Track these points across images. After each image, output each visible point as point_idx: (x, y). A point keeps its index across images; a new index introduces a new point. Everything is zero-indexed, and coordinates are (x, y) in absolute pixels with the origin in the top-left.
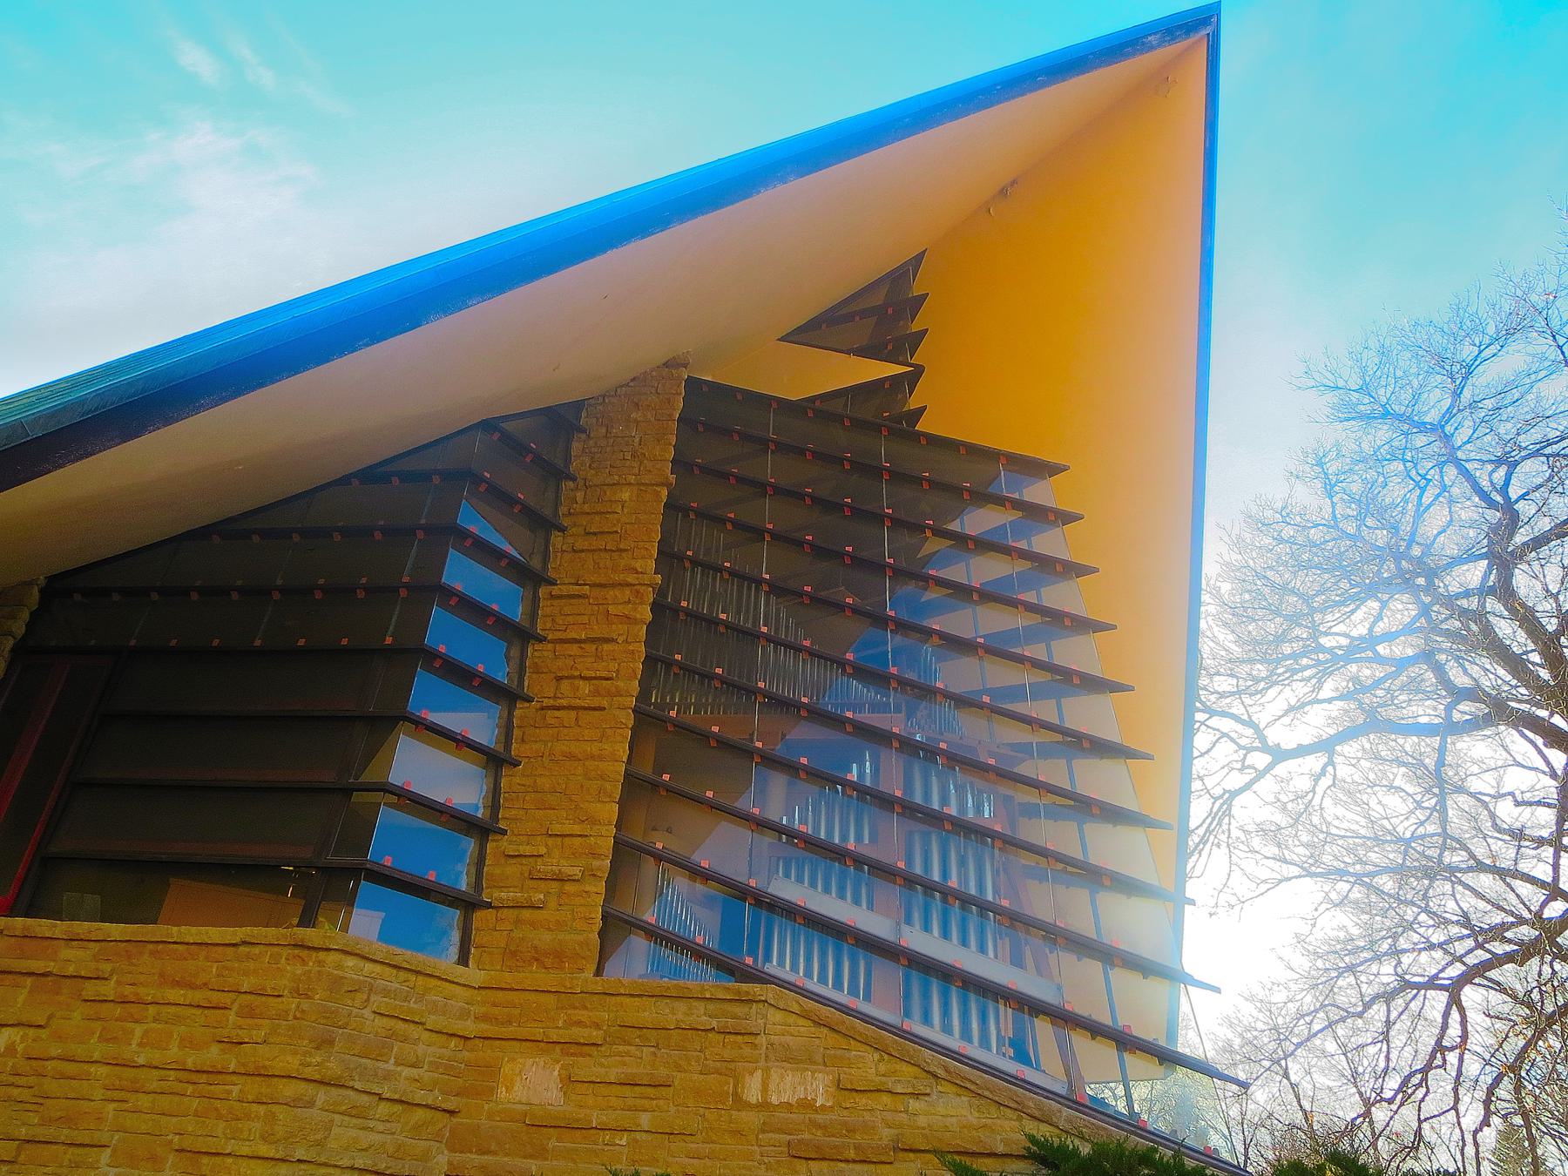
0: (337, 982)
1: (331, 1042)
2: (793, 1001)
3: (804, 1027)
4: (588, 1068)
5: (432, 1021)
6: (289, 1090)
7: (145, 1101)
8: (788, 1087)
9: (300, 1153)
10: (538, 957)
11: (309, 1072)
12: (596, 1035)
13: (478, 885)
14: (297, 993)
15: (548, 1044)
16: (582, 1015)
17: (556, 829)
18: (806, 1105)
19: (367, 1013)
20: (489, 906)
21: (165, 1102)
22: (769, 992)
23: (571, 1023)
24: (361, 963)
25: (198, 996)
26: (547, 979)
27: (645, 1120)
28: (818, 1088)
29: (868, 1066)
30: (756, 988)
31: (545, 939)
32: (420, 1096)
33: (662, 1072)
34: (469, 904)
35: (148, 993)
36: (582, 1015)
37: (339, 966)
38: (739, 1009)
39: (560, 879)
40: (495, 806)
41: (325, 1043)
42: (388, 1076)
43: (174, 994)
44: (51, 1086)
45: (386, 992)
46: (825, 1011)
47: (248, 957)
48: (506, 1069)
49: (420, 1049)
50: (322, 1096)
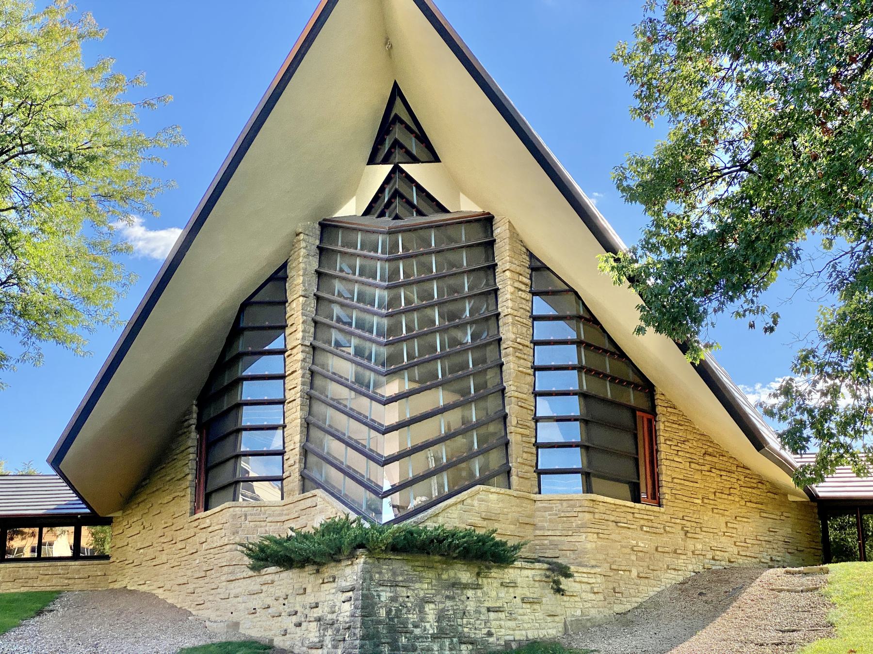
0: (234, 516)
1: (238, 533)
5: (267, 520)
6: (228, 547)
9: (234, 563)
11: (231, 542)
12: (296, 515)
19: (247, 522)
24: (240, 509)
34: (281, 479)
36: (297, 509)
37: (234, 511)
38: (313, 498)
41: (235, 533)
45: (251, 515)
47: (223, 514)
49: (267, 529)
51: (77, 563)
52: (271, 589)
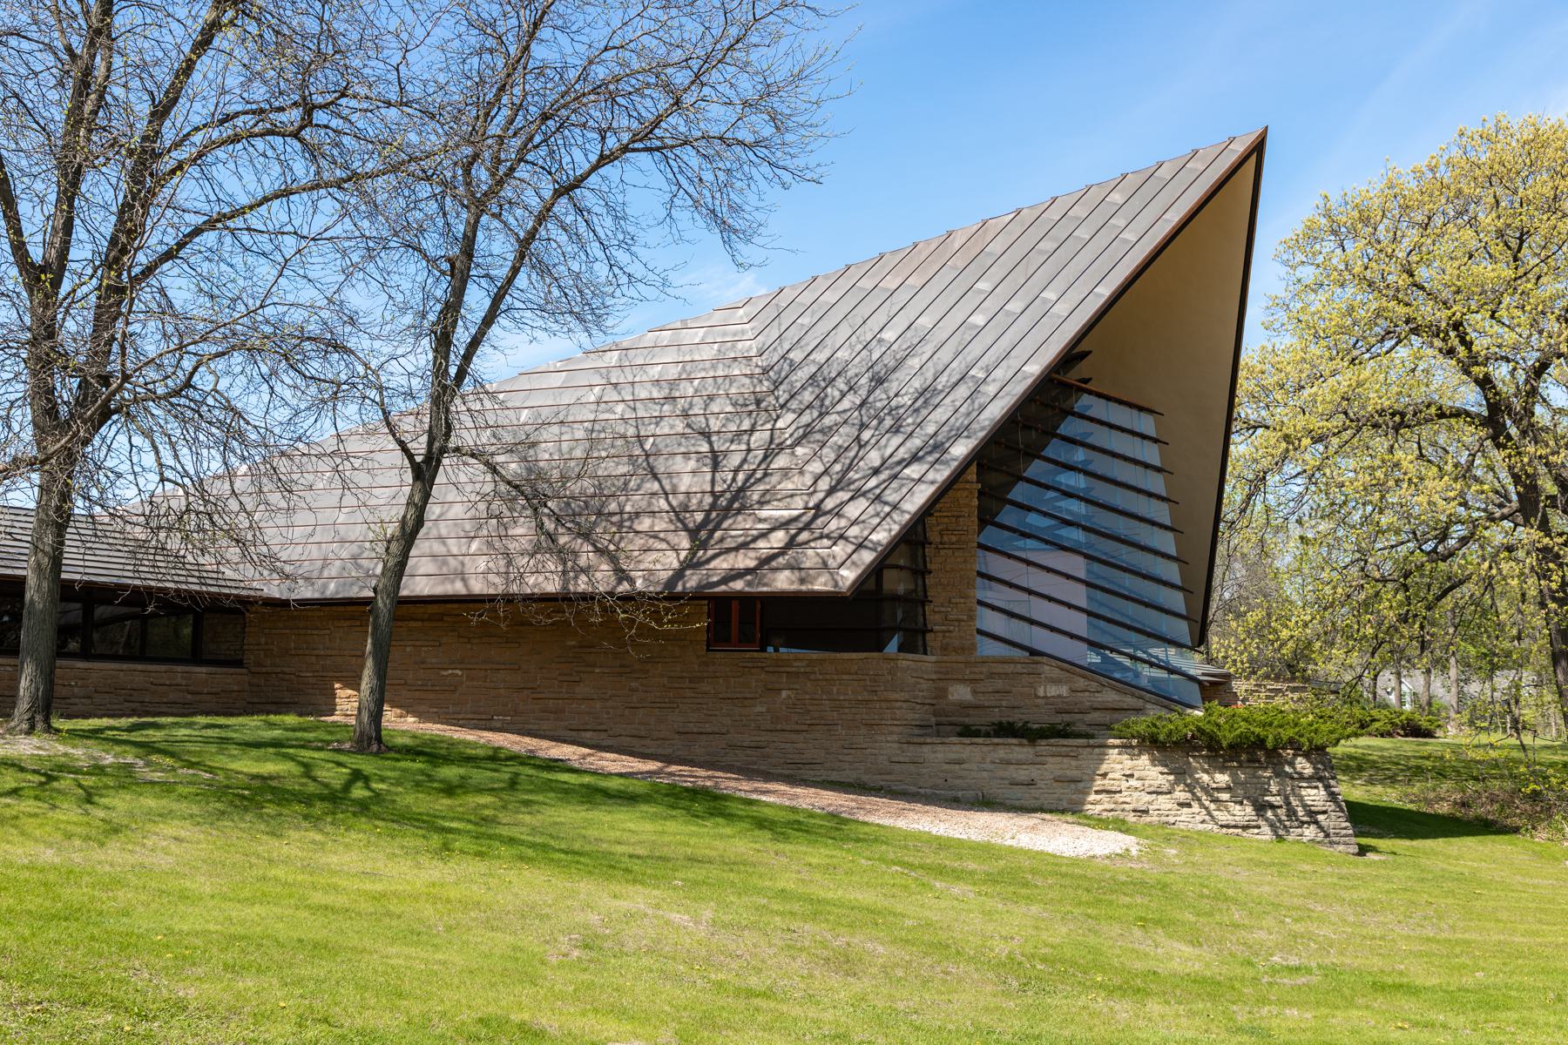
2: (1054, 662)
3: (1057, 671)
4: (980, 687)
7: (847, 711)
8: (1053, 691)
10: (955, 650)
13: (925, 624)
14: (890, 673)
15: (963, 681)
16: (976, 670)
17: (953, 600)
18: (1060, 696)
20: (931, 631)
21: (854, 710)
22: (1045, 659)
23: (971, 673)
25: (855, 677)
26: (961, 658)
27: (1004, 703)
28: (1064, 690)
29: (1081, 683)
30: (1036, 658)
31: (957, 643)
32: (927, 701)
33: (1008, 688)
35: (835, 677)
36: (976, 670)
39: (959, 621)
40: (925, 591)
42: (917, 697)
43: (844, 677)
44: (811, 708)
46: (1066, 665)
48: (950, 689)
50: (905, 705)
51: (204, 669)
52: (1074, 763)
